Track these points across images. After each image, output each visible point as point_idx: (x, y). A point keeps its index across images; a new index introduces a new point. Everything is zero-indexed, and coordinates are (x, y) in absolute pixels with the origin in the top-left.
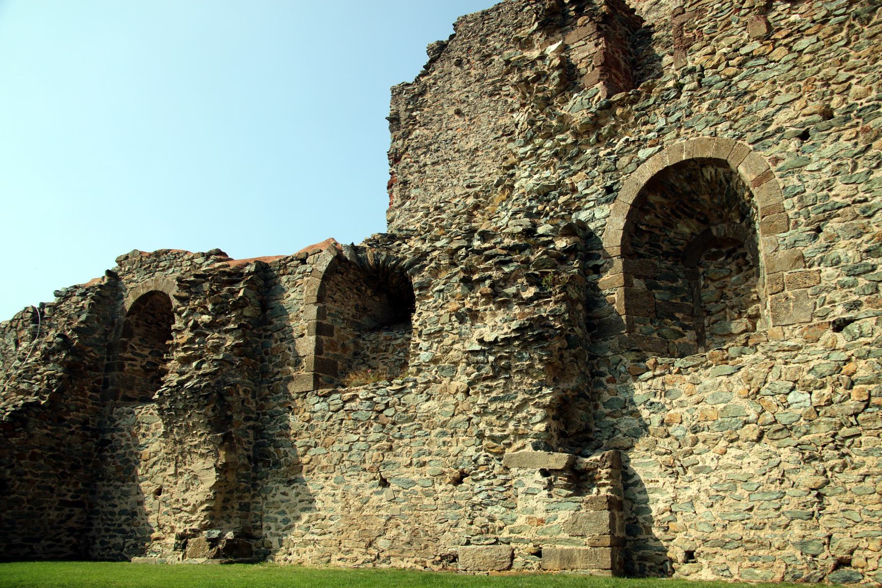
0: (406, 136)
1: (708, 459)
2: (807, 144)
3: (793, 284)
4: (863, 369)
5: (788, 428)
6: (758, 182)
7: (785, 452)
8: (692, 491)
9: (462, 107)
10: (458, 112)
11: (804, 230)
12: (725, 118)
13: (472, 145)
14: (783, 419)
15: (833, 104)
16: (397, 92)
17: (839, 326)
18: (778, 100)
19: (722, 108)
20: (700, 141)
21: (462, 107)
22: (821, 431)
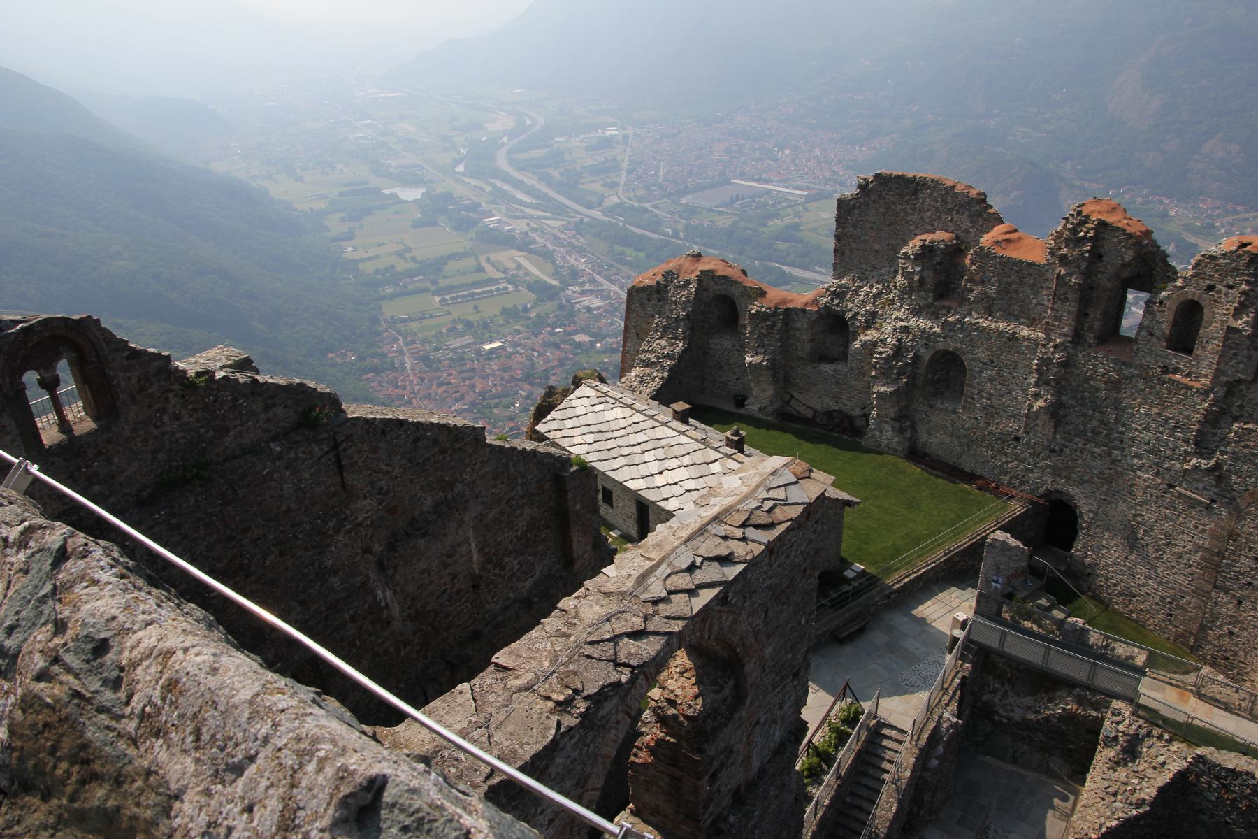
0: (844, 228)
13: (876, 247)
16: (841, 202)
22: (965, 441)
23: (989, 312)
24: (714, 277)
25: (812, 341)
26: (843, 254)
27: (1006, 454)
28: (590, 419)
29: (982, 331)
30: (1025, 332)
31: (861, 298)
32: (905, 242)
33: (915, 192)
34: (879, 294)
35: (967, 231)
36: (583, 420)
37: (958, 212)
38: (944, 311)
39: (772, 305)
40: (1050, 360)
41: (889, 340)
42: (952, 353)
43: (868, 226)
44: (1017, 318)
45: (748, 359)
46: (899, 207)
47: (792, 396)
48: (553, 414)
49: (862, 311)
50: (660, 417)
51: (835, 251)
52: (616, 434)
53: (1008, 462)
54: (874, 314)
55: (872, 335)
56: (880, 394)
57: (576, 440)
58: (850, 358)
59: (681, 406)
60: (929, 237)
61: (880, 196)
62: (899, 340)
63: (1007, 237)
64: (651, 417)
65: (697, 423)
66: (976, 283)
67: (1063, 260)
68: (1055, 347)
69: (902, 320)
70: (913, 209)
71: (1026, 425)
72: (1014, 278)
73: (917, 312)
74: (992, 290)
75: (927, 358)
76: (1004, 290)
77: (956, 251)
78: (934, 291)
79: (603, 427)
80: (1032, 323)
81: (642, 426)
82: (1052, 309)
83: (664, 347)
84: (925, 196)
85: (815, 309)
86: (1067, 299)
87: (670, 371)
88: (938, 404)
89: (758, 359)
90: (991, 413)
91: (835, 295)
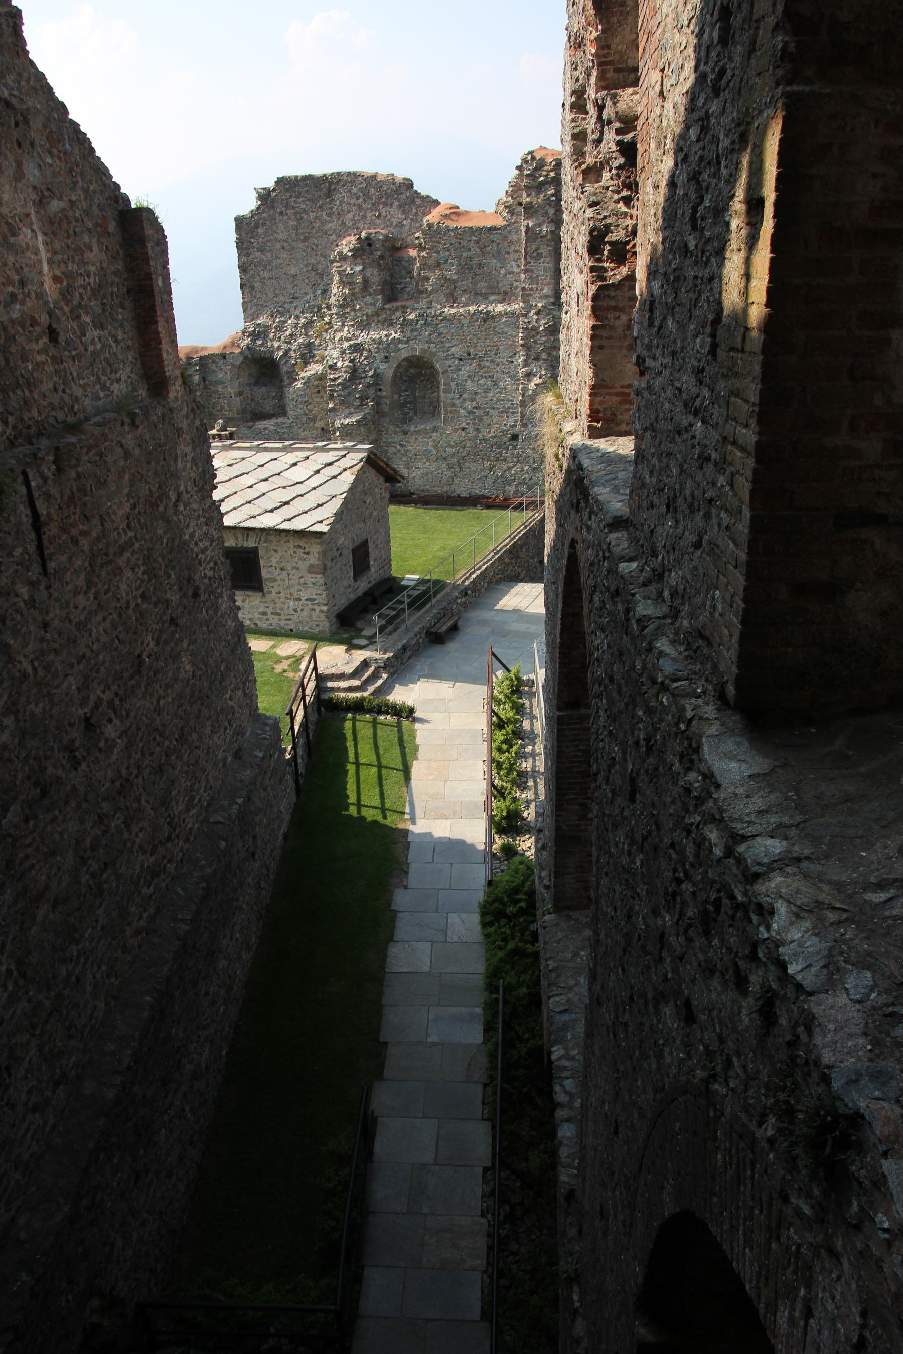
0: (248, 255)
1: (420, 465)
2: (461, 363)
3: (451, 412)
4: (468, 444)
5: (445, 459)
6: (443, 373)
7: (444, 466)
8: (414, 475)
9: (285, 244)
10: (283, 248)
11: (458, 396)
12: (434, 342)
13: (293, 271)
14: (444, 456)
15: (472, 350)
16: (240, 221)
17: (463, 429)
18: (454, 342)
19: (433, 337)
20: (424, 349)
21: (285, 244)
22: (455, 460)
23: (453, 299)
25: (240, 394)
26: (252, 287)
27: (505, 460)
30: (500, 308)
33: (329, 194)
34: (309, 324)
35: (400, 225)
37: (385, 204)
38: (398, 314)
40: (535, 329)
41: (339, 364)
42: (419, 358)
43: (278, 246)
44: (485, 296)
46: (312, 215)
51: (242, 286)
53: (509, 469)
54: (309, 346)
55: (315, 368)
58: (290, 405)
61: (287, 206)
62: (351, 361)
67: (530, 210)
68: (538, 313)
69: (348, 340)
70: (330, 215)
71: (523, 416)
72: (475, 250)
73: (363, 326)
74: (451, 273)
75: (390, 373)
76: (466, 267)
78: (382, 292)
80: (505, 297)
82: (526, 271)
84: (341, 195)
85: (237, 351)
86: (540, 255)
88: (412, 428)
90: (479, 415)
91: (255, 336)
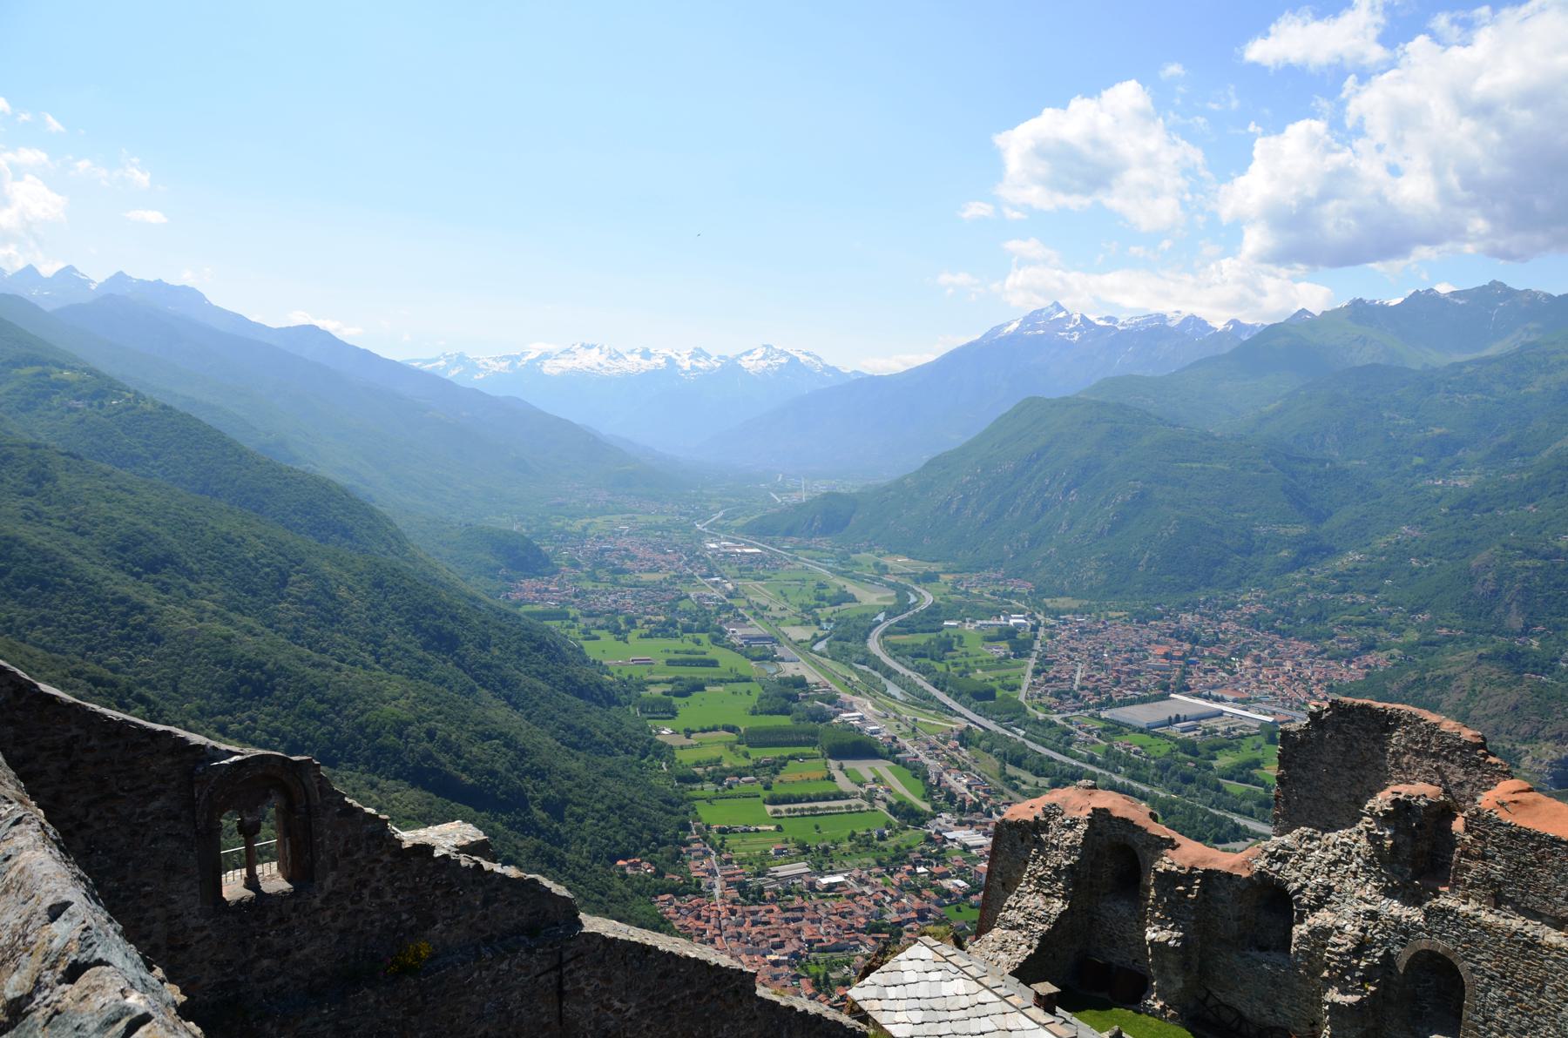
13: (1334, 797)
23: (1498, 901)
24: (1110, 817)
28: (922, 990)
29: (1486, 928)
31: (1311, 865)
32: (1372, 794)
36: (912, 991)
39: (1187, 865)
41: (1349, 928)
45: (1150, 935)
47: (1209, 993)
48: (873, 977)
49: (1312, 884)
50: (1014, 1000)
52: (952, 1016)
55: (1323, 918)
56: (1333, 1005)
57: (899, 1017)
59: (1046, 988)
60: (1404, 790)
63: (1517, 797)
64: (1003, 998)
65: (1067, 1015)
66: (1473, 858)
69: (1366, 901)
73: (1389, 893)
76: (1517, 872)
77: (1445, 812)
79: (937, 1004)
81: (988, 1009)
83: (1035, 905)
87: (1042, 939)
89: (1163, 936)
